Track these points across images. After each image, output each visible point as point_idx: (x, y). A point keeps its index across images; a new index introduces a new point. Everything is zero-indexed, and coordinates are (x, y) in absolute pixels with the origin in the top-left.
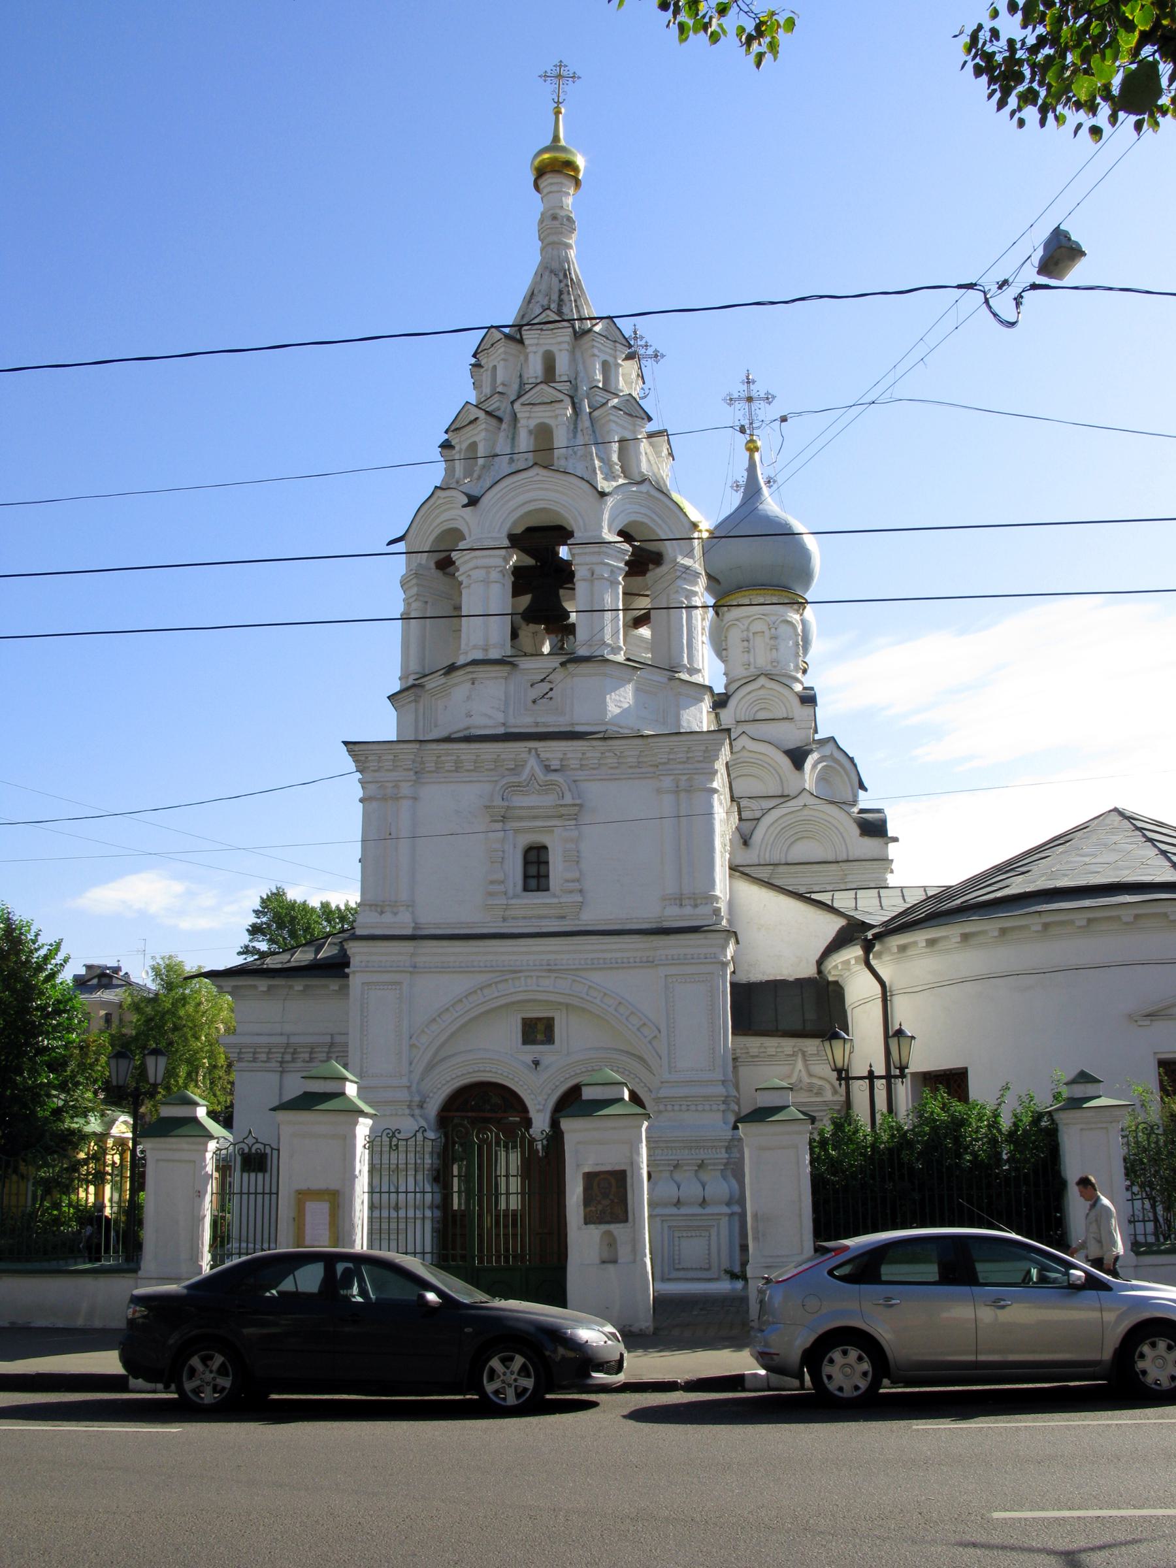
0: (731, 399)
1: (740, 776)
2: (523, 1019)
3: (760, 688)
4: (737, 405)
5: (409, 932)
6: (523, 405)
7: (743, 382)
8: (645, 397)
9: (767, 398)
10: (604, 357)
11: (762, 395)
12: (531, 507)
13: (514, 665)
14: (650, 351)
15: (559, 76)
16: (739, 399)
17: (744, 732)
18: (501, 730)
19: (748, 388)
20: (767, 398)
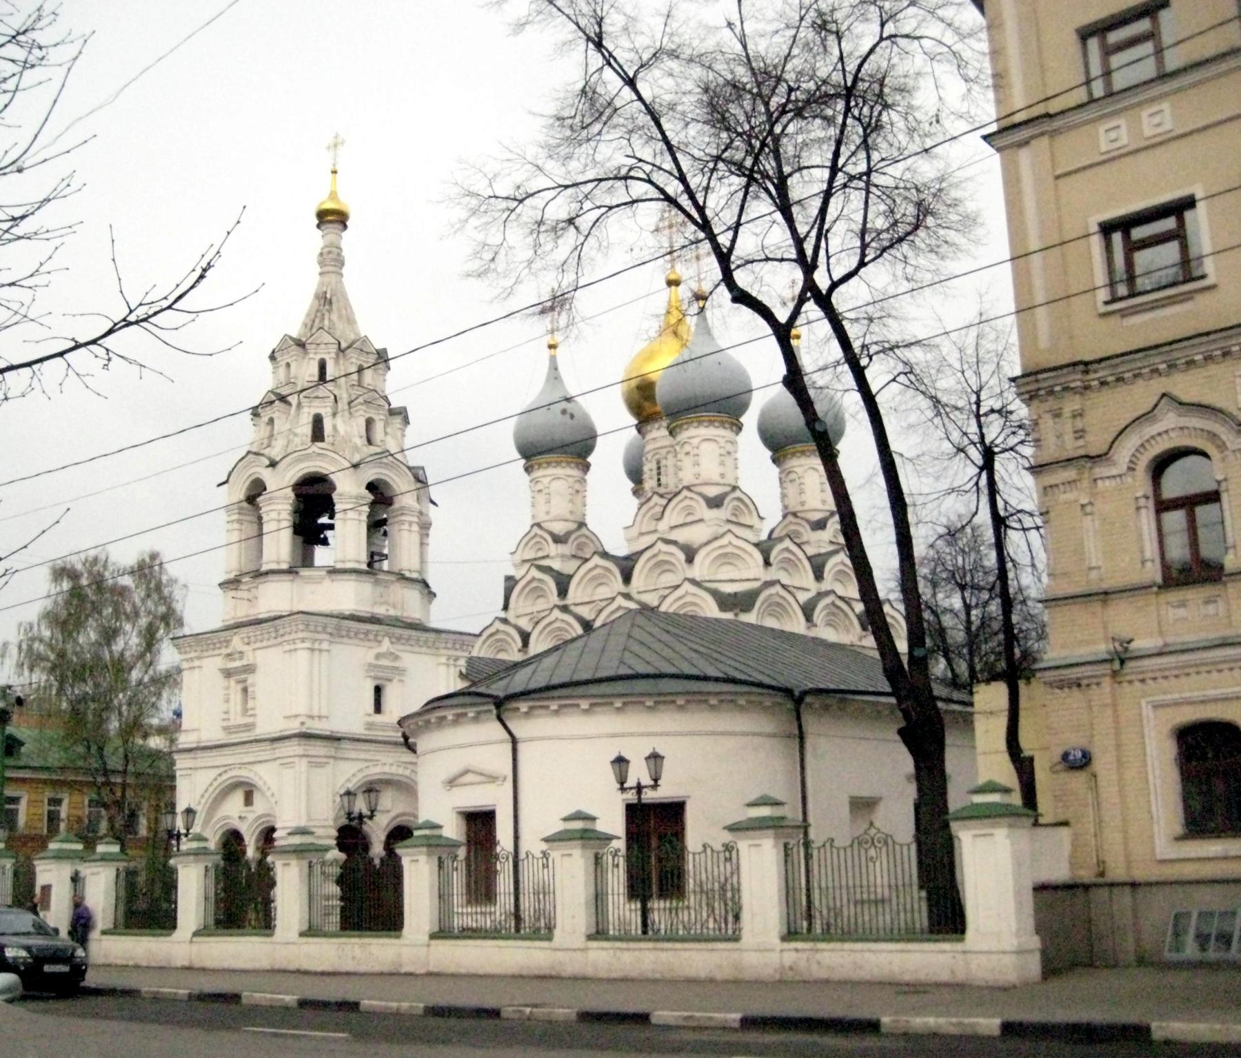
5: (194, 745)
10: (318, 357)
18: (232, 622)
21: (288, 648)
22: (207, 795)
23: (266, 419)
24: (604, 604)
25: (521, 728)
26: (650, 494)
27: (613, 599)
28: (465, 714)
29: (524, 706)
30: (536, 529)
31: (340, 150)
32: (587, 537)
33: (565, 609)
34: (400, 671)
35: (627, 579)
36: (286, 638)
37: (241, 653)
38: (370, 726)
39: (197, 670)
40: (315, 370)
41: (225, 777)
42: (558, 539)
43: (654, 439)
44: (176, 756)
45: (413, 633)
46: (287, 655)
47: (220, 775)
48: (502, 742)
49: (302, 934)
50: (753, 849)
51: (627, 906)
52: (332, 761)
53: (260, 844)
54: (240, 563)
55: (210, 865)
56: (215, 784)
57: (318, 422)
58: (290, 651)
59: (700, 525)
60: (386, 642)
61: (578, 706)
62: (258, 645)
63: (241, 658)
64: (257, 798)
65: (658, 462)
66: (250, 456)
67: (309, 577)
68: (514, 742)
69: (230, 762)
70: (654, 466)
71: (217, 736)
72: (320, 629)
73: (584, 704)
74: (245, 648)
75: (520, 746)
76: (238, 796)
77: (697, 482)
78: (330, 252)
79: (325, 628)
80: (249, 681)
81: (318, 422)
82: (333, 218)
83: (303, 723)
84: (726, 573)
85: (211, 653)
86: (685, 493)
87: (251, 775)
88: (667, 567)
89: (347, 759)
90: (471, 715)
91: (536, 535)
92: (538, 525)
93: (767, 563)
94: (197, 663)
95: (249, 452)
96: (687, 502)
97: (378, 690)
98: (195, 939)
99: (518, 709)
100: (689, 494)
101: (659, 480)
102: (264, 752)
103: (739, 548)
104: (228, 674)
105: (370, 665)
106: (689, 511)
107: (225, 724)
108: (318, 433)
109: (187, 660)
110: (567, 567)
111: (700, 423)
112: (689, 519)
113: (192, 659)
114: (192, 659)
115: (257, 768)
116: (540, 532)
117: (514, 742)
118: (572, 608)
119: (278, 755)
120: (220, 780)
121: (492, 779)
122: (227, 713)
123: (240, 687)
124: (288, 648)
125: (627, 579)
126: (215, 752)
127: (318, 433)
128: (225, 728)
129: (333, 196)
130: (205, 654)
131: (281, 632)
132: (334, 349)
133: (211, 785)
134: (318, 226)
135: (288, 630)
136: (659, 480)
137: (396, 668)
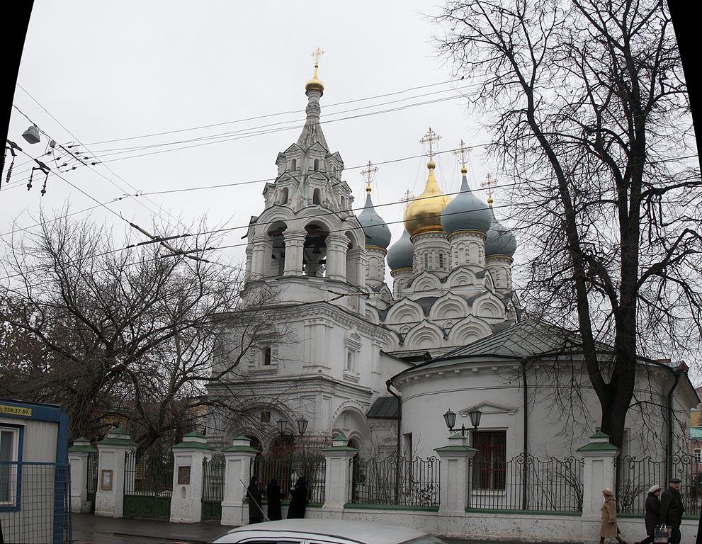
10: (315, 158)
14: (436, 136)
15: (318, 54)
24: (412, 326)
26: (420, 272)
27: (420, 323)
31: (321, 56)
32: (386, 291)
33: (384, 327)
34: (359, 345)
35: (426, 313)
36: (305, 318)
38: (346, 377)
40: (312, 164)
42: (376, 290)
43: (424, 243)
45: (366, 325)
50: (452, 463)
52: (332, 396)
54: (263, 269)
55: (209, 459)
57: (316, 193)
60: (355, 327)
65: (426, 255)
66: (275, 207)
67: (313, 283)
70: (424, 256)
77: (468, 264)
78: (315, 106)
79: (332, 313)
81: (316, 193)
82: (314, 89)
83: (320, 371)
84: (486, 314)
86: (461, 269)
89: (337, 396)
95: (275, 205)
98: (346, 510)
103: (494, 301)
105: (349, 340)
106: (463, 279)
107: (252, 369)
108: (316, 200)
110: (383, 306)
111: (470, 234)
112: (463, 284)
121: (506, 410)
124: (307, 323)
125: (426, 313)
127: (316, 200)
129: (315, 77)
132: (323, 155)
135: (311, 312)
137: (359, 344)
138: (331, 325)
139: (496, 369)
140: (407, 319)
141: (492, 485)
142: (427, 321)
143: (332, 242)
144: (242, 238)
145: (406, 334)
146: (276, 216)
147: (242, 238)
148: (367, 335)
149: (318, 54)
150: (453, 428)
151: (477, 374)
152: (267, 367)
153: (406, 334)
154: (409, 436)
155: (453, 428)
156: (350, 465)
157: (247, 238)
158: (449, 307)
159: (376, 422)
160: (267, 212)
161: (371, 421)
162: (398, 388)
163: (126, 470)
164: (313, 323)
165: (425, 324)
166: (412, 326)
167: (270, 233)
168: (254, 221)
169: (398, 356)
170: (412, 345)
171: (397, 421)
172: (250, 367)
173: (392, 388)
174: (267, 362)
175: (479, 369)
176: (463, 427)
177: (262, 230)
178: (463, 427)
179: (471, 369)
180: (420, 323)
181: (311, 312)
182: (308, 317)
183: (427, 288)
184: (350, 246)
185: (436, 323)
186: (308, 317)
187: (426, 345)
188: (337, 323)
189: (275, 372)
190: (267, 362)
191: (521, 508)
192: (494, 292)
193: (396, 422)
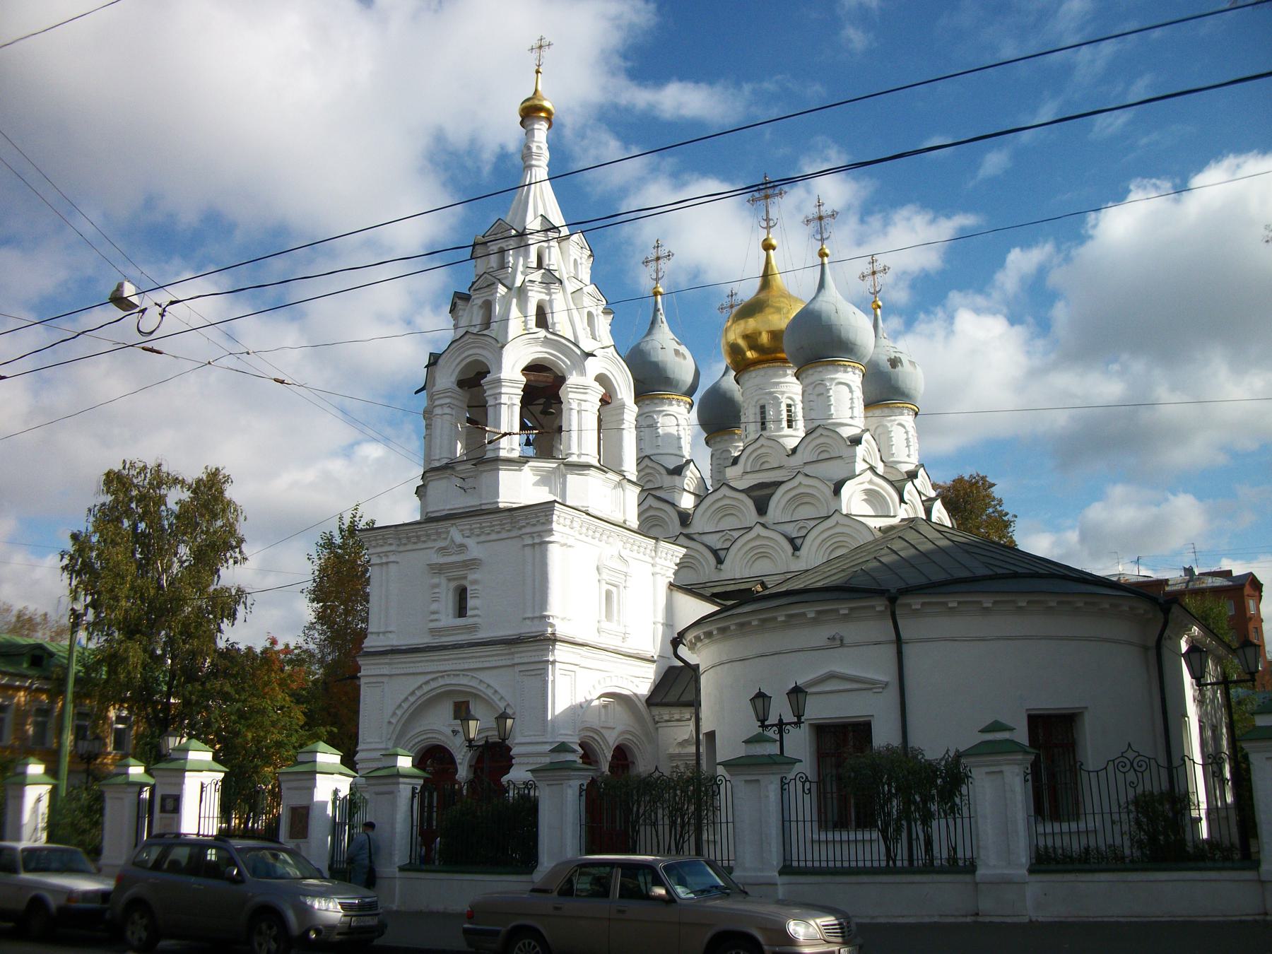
0: (807, 221)
1: (802, 504)
2: (455, 702)
3: (819, 437)
4: (812, 224)
6: (475, 290)
7: (815, 206)
8: (775, 225)
9: (833, 215)
11: (830, 213)
12: (468, 360)
13: (453, 468)
15: (541, 47)
16: (814, 219)
17: (724, 484)
19: (819, 210)
20: (833, 215)
21: (529, 542)
22: (405, 705)
23: (479, 302)
25: (909, 628)
27: (751, 528)
28: (749, 623)
29: (916, 602)
30: (646, 461)
31: (546, 53)
33: (689, 537)
35: (762, 509)
36: (524, 531)
37: (462, 545)
39: (391, 566)
41: (433, 685)
44: (361, 661)
46: (528, 551)
47: (427, 683)
48: (890, 642)
49: (781, 873)
51: (1040, 829)
53: (473, 763)
56: (418, 693)
58: (533, 545)
59: (838, 462)
61: (945, 604)
62: (483, 538)
63: (460, 553)
64: (475, 709)
65: (763, 407)
68: (899, 642)
69: (441, 668)
70: (758, 410)
71: (424, 640)
72: (568, 522)
73: (988, 602)
74: (471, 542)
75: (907, 649)
76: (447, 710)
80: (471, 577)
85: (409, 547)
87: (474, 683)
88: (806, 500)
90: (755, 623)
91: (647, 466)
92: (648, 457)
93: (902, 500)
94: (392, 558)
96: (821, 440)
97: (609, 595)
99: (909, 605)
100: (825, 433)
101: (763, 424)
102: (495, 657)
104: (438, 569)
107: (432, 625)
108: (542, 320)
109: (378, 554)
113: (386, 554)
114: (386, 554)
115: (481, 675)
116: (650, 464)
117: (899, 642)
118: (695, 537)
119: (516, 661)
120: (426, 688)
121: (871, 686)
122: (433, 613)
123: (453, 585)
125: (762, 509)
126: (386, 659)
127: (542, 320)
128: (433, 631)
130: (401, 549)
131: (522, 523)
133: (413, 693)
134: (522, 123)
136: (763, 424)
138: (570, 541)
139: (846, 612)
140: (727, 523)
141: (853, 823)
142: (763, 525)
143: (571, 395)
144: (416, 393)
145: (728, 549)
146: (466, 354)
147: (416, 393)
148: (641, 556)
149: (541, 47)
150: (766, 723)
151: (815, 621)
152: (461, 621)
153: (728, 549)
154: (711, 736)
155: (766, 723)
156: (580, 795)
157: (425, 391)
158: (799, 500)
159: (665, 713)
160: (456, 344)
161: (656, 711)
162: (692, 647)
163: (202, 815)
164: (537, 541)
165: (758, 530)
166: (736, 534)
167: (461, 383)
168: (434, 360)
169: (708, 592)
170: (738, 568)
171: (693, 710)
172: (432, 621)
173: (683, 651)
174: (462, 610)
175: (819, 612)
176: (781, 720)
177: (447, 379)
178: (781, 720)
179: (804, 614)
180: (751, 528)
181: (533, 521)
182: (528, 530)
183: (766, 466)
184: (604, 401)
185: (779, 528)
186: (528, 530)
187: (762, 568)
188: (583, 537)
189: (473, 628)
190: (462, 610)
191: (906, 863)
192: (881, 469)
193: (687, 713)
